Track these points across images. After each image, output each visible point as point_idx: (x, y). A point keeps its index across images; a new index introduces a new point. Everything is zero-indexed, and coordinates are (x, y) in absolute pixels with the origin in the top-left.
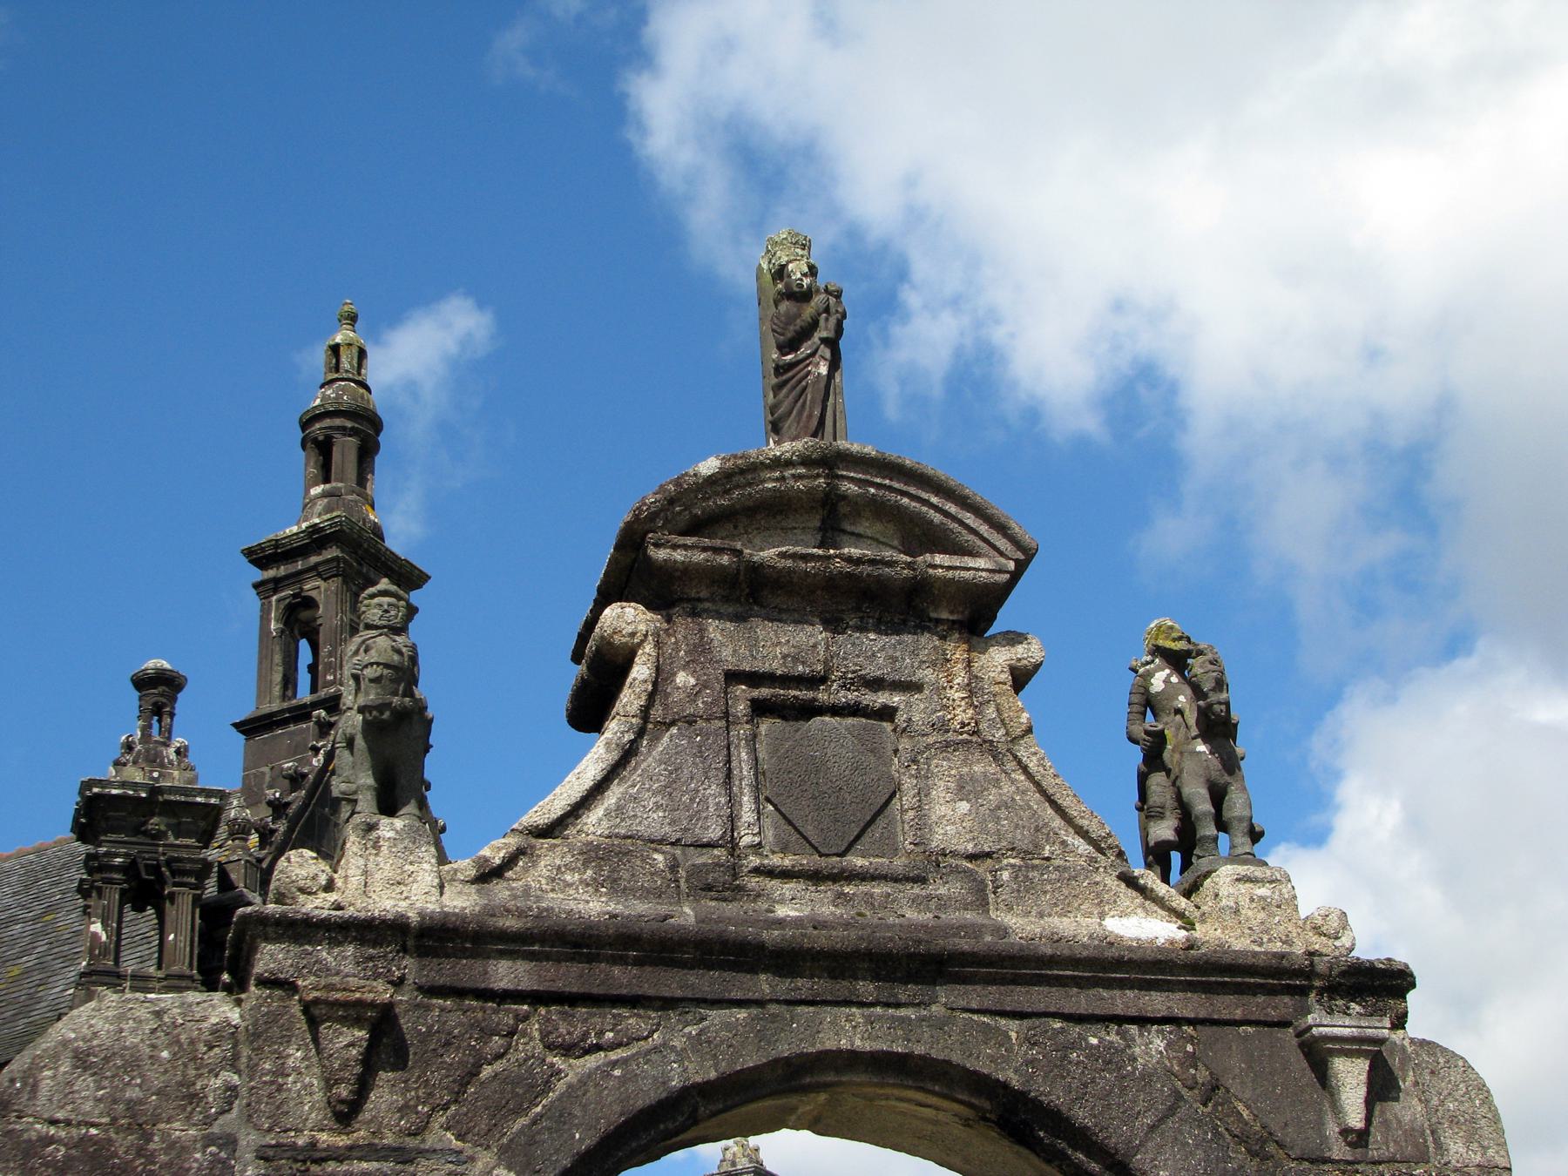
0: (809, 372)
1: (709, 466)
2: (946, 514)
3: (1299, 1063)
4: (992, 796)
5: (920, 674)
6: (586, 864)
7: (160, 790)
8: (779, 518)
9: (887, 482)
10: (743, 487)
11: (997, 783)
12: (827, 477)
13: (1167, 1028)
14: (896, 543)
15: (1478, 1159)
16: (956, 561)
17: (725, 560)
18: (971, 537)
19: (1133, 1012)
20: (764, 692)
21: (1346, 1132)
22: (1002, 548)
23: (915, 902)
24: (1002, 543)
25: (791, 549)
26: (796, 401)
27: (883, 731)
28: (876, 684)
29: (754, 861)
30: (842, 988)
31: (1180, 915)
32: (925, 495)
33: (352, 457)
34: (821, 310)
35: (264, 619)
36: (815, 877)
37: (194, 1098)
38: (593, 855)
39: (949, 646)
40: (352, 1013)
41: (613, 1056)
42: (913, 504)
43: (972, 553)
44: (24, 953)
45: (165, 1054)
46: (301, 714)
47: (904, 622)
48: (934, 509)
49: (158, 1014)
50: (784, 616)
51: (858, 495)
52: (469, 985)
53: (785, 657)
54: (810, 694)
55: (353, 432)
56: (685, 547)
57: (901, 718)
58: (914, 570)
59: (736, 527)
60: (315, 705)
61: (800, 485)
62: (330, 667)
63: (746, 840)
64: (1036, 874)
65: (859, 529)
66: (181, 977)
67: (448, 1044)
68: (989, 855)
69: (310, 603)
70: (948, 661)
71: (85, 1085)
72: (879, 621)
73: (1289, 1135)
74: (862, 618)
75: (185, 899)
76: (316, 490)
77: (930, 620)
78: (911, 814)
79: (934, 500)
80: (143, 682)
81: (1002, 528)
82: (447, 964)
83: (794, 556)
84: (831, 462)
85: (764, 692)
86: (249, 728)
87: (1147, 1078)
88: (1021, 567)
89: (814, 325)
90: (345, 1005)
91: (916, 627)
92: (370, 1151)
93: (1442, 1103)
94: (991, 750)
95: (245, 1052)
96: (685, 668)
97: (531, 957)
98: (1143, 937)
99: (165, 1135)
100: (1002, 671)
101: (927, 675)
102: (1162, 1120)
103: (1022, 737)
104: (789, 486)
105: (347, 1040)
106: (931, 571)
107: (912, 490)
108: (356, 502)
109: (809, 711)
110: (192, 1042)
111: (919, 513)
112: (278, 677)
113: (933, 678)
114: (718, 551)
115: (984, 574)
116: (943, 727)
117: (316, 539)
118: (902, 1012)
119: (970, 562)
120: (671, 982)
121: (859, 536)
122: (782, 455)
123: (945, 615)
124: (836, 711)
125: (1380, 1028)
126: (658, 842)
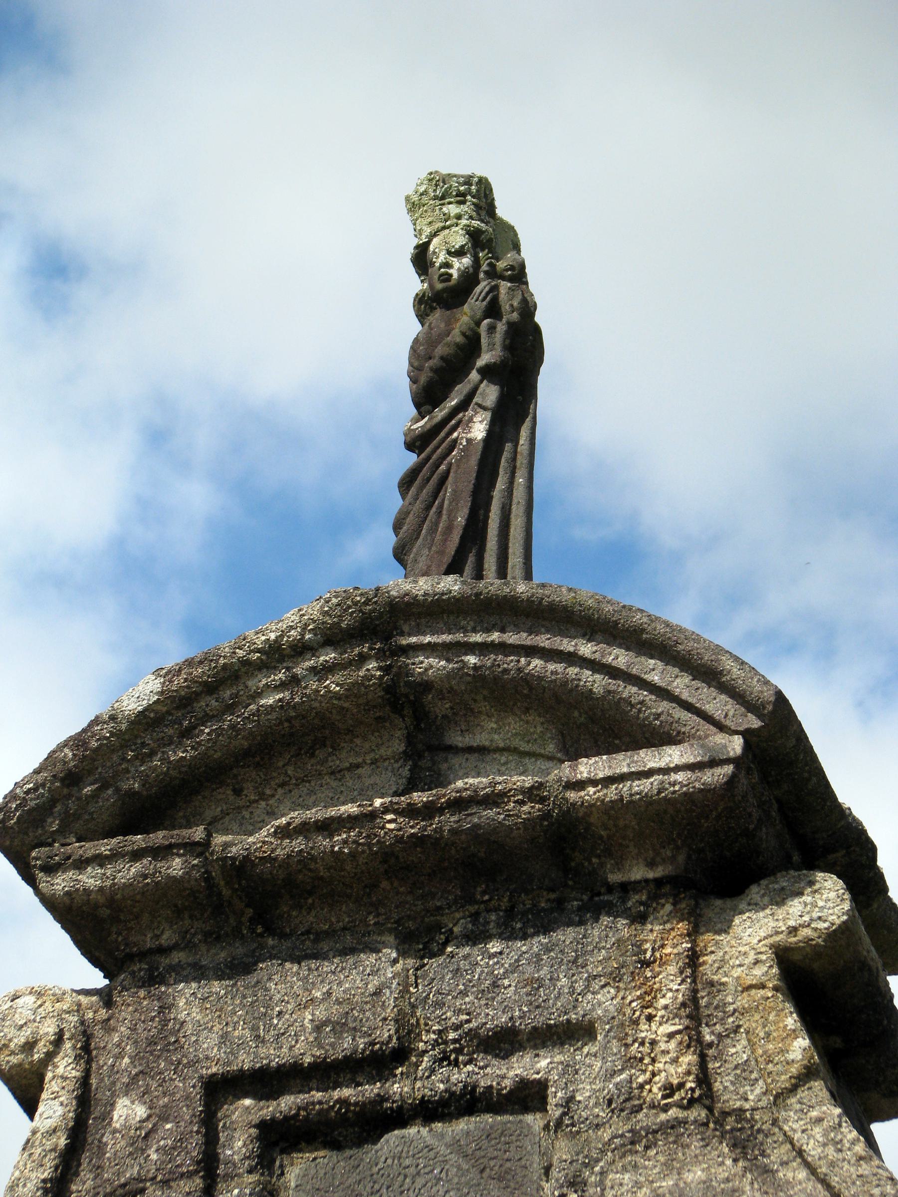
0: (455, 441)
2: (613, 672)
5: (585, 1005)
8: (320, 754)
9: (495, 636)
10: (217, 716)
12: (380, 655)
14: (551, 748)
16: (622, 763)
17: (176, 866)
18: (664, 706)
20: (287, 1103)
22: (718, 715)
25: (296, 816)
26: (428, 507)
32: (567, 645)
34: (479, 314)
39: (652, 932)
42: (551, 667)
47: (560, 904)
50: (325, 946)
51: (450, 675)
53: (318, 1028)
54: (371, 1090)
56: (100, 860)
57: (556, 1096)
58: (542, 800)
59: (238, 792)
61: (332, 684)
65: (480, 739)
70: (647, 964)
72: (511, 913)
74: (475, 916)
77: (610, 889)
79: (586, 649)
83: (304, 829)
85: (287, 1103)
91: (581, 909)
96: (127, 1090)
100: (757, 962)
103: (793, 1089)
104: (308, 691)
106: (572, 795)
107: (544, 640)
111: (565, 683)
113: (611, 1006)
114: (160, 852)
115: (680, 777)
119: (650, 759)
121: (482, 750)
122: (282, 636)
123: (638, 873)
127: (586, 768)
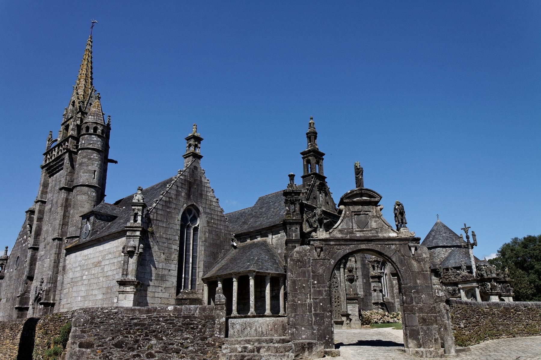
1: (349, 192)
7: (293, 190)
21: (412, 254)
23: (370, 233)
24: (379, 197)
28: (366, 211)
29: (355, 230)
30: (363, 243)
31: (397, 233)
33: (314, 139)
35: (304, 162)
36: (361, 231)
37: (306, 255)
40: (319, 247)
43: (376, 198)
44: (277, 208)
46: (310, 175)
48: (372, 193)
55: (313, 135)
60: (311, 174)
62: (313, 169)
66: (298, 214)
69: (310, 160)
71: (297, 254)
73: (406, 255)
75: (297, 204)
76: (309, 144)
80: (289, 176)
81: (378, 195)
82: (327, 242)
84: (361, 189)
85: (355, 213)
86: (303, 177)
87: (393, 250)
88: (381, 199)
89: (360, 172)
94: (378, 217)
101: (372, 210)
105: (319, 250)
109: (360, 214)
112: (306, 170)
116: (373, 215)
117: (309, 151)
120: (347, 243)
124: (363, 214)
125: (416, 245)
126: (345, 229)
127: (372, 199)
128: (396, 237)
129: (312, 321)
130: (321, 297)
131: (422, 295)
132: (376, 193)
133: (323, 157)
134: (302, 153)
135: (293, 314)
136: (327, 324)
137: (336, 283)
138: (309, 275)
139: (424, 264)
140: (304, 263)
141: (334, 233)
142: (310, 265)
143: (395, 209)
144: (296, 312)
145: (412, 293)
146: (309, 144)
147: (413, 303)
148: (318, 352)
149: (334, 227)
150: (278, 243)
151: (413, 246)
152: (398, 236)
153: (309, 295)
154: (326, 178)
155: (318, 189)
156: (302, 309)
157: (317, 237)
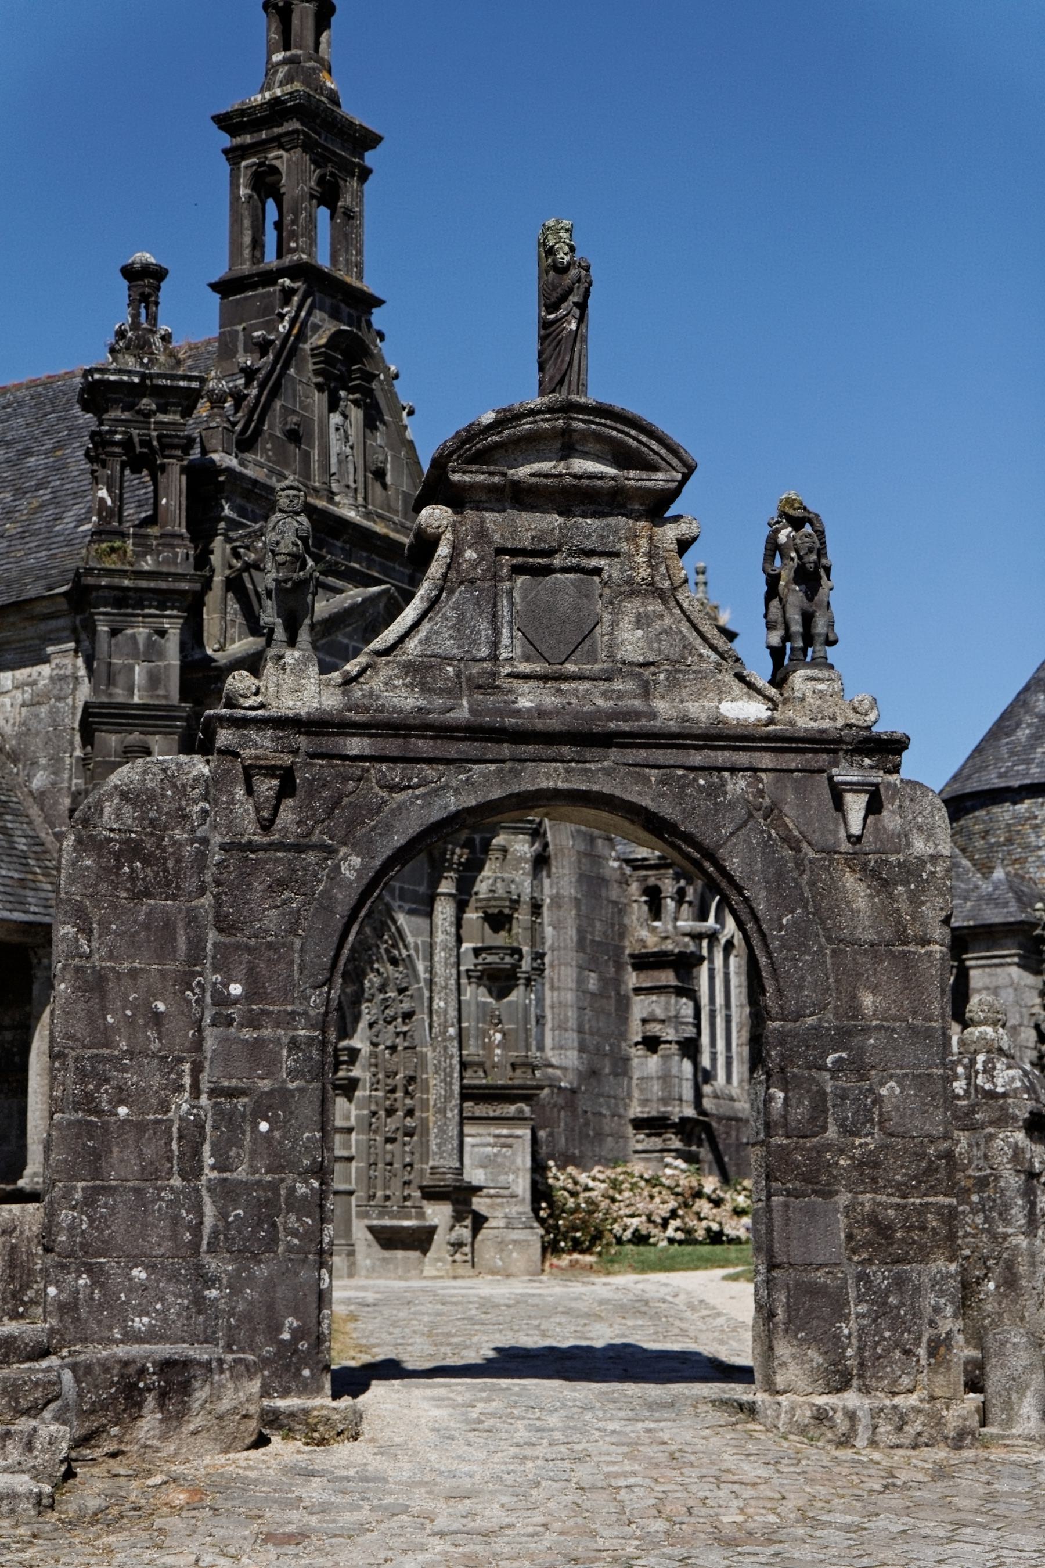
1: (488, 417)
2: (640, 442)
3: (827, 795)
4: (657, 626)
6: (407, 674)
7: (151, 376)
11: (661, 617)
13: (749, 774)
15: (931, 851)
17: (496, 479)
18: (655, 457)
19: (728, 765)
21: (849, 837)
23: (604, 694)
24: (675, 462)
27: (594, 582)
28: (591, 553)
29: (507, 670)
30: (552, 751)
31: (770, 699)
32: (627, 430)
33: (310, 23)
35: (234, 185)
36: (544, 678)
37: (186, 817)
38: (409, 668)
40: (270, 771)
41: (417, 792)
43: (655, 468)
44: (39, 486)
45: (169, 793)
46: (269, 278)
48: (631, 439)
49: (164, 771)
52: (335, 752)
56: (471, 472)
60: (282, 272)
61: (546, 425)
62: (294, 236)
63: (504, 655)
64: (681, 676)
65: (586, 449)
66: (174, 535)
67: (324, 785)
68: (652, 664)
69: (275, 171)
71: (127, 810)
73: (815, 837)
75: (175, 467)
76: (277, 57)
78: (606, 638)
80: (129, 273)
81: (674, 450)
84: (569, 408)
85: (520, 560)
86: (224, 288)
87: (732, 805)
88: (686, 478)
89: (570, 291)
90: (266, 767)
92: (280, 846)
93: (914, 818)
94: (661, 595)
95: (212, 791)
97: (371, 736)
98: (741, 717)
99: (171, 837)
101: (624, 547)
102: (738, 829)
105: (267, 786)
107: (619, 426)
108: (314, 69)
110: (183, 786)
112: (247, 240)
114: (492, 474)
116: (630, 581)
117: (277, 111)
118: (587, 765)
120: (453, 749)
125: (878, 777)
126: (448, 659)
127: (632, 474)
128: (759, 723)
129: (197, 1229)
130: (265, 1085)
131: (882, 1084)
132: (661, 440)
133: (370, 158)
134: (226, 122)
135: (81, 1185)
136: (290, 1248)
137: (401, 991)
138: (196, 946)
139: (915, 900)
140: (170, 864)
141: (375, 682)
142: (208, 878)
143: (773, 547)
144: (96, 1173)
145: (823, 1068)
146: (277, 57)
147: (825, 1129)
148: (220, 1418)
149: (378, 644)
150: (33, 724)
151: (857, 788)
152: (771, 721)
153: (187, 1067)
154: (379, 302)
155: (317, 373)
156: (140, 1155)
157: (262, 706)
